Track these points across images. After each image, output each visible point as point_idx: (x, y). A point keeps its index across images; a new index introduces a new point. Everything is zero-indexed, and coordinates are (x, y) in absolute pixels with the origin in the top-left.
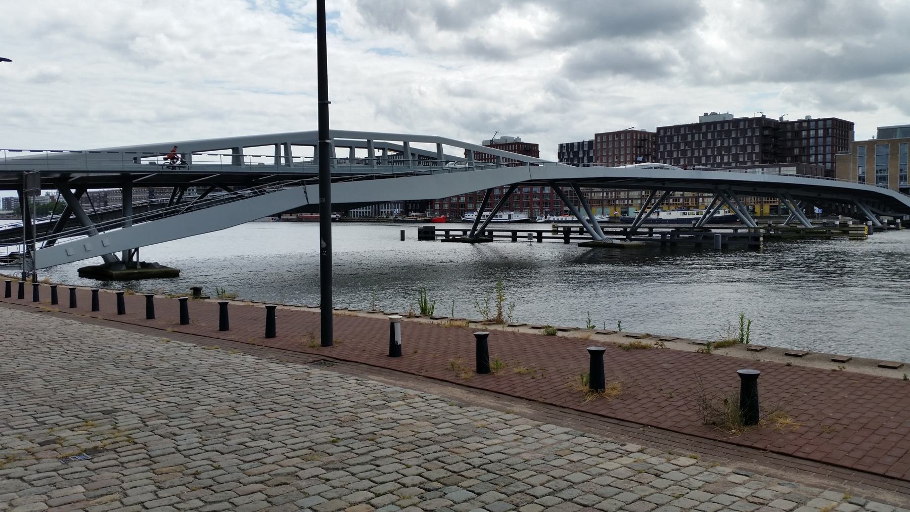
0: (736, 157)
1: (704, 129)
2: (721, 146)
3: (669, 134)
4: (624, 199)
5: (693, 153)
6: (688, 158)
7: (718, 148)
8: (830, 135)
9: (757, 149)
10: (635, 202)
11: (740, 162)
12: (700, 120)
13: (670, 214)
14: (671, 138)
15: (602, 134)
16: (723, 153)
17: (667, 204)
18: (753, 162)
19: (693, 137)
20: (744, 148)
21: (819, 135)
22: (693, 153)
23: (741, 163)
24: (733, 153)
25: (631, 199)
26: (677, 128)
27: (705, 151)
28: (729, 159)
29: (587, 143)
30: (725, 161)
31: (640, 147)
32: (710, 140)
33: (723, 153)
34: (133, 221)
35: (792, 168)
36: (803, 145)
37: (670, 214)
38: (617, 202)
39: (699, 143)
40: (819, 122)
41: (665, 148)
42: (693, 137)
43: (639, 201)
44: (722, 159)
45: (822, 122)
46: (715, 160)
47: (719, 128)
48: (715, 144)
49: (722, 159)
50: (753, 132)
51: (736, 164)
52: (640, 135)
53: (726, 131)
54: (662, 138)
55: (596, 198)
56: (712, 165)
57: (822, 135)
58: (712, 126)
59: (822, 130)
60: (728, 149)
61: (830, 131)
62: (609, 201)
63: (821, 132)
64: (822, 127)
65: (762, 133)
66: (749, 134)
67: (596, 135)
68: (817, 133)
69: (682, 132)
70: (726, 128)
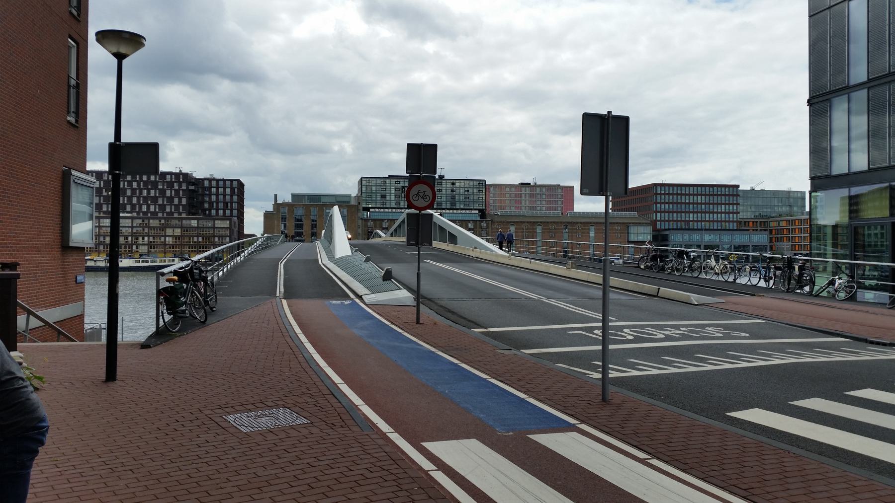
7: (144, 197)
8: (236, 193)
9: (184, 201)
11: (167, 213)
16: (149, 202)
17: (96, 251)
18: (180, 214)
20: (170, 200)
24: (159, 203)
28: (171, 209)
30: (151, 210)
32: (135, 189)
33: (149, 202)
36: (212, 200)
44: (148, 208)
45: (229, 182)
46: (141, 208)
48: (141, 193)
49: (148, 208)
50: (180, 186)
51: (163, 213)
53: (152, 182)
56: (138, 213)
59: (229, 189)
60: (155, 200)
61: (236, 190)
63: (228, 191)
65: (187, 187)
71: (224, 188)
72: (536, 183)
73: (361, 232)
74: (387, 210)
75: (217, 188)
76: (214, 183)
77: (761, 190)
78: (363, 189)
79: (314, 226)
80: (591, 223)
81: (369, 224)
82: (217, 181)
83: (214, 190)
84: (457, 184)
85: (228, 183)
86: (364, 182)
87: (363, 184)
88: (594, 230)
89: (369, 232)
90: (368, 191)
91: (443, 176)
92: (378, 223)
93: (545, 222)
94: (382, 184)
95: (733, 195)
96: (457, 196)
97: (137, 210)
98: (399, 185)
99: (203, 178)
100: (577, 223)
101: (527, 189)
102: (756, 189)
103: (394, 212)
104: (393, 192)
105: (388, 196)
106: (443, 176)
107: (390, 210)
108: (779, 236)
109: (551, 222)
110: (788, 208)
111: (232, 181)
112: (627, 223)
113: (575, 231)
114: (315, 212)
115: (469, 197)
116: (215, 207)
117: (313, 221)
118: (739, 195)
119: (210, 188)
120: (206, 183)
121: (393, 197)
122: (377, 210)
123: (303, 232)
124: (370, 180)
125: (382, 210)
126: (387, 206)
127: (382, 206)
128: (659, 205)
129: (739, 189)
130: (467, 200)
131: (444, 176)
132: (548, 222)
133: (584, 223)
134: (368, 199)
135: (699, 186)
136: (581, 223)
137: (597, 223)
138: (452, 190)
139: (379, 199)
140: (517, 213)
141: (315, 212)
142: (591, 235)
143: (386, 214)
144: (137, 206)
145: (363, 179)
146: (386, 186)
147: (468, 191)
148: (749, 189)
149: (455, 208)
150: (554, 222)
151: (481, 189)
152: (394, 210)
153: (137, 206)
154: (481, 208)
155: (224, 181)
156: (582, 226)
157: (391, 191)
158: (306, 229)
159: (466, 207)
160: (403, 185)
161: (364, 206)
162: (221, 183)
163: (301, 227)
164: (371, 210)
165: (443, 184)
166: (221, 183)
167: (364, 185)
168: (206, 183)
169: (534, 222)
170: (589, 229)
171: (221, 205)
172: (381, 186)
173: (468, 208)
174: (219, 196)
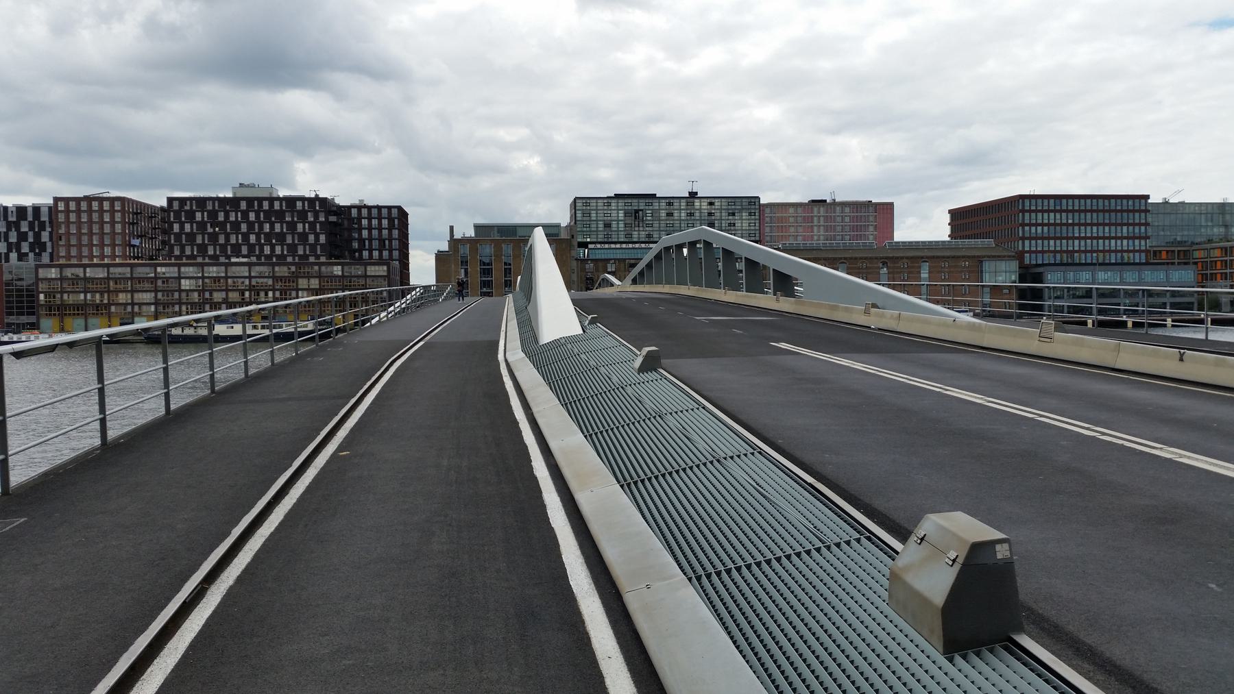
0: (203, 249)
1: (243, 205)
2: (270, 232)
3: (187, 208)
4: (126, 305)
5: (227, 239)
6: (310, 245)
7: (266, 234)
8: (396, 226)
9: (323, 238)
10: (144, 308)
11: (300, 256)
12: (234, 193)
13: (232, 327)
14: (191, 216)
15: (68, 198)
16: (274, 241)
18: (318, 257)
19: (227, 216)
20: (303, 237)
21: (383, 226)
22: (227, 239)
23: (211, 257)
25: (136, 304)
26: (201, 202)
27: (246, 237)
28: (305, 250)
29: (14, 209)
30: (277, 253)
31: (133, 224)
34: (1041, 298)
35: (381, 268)
36: (364, 237)
37: (232, 327)
38: (113, 309)
39: (236, 226)
40: (383, 210)
41: (182, 228)
42: (227, 216)
43: (153, 308)
44: (273, 250)
45: (386, 209)
46: (262, 250)
47: (266, 205)
48: (261, 228)
49: (273, 250)
50: (316, 216)
52: (137, 205)
54: (178, 214)
55: (71, 302)
56: (259, 257)
57: (387, 226)
58: (256, 203)
59: (386, 220)
60: (281, 238)
61: (396, 221)
62: (97, 307)
63: (385, 223)
64: (376, 216)
65: (327, 218)
66: (311, 219)
67: (56, 200)
68: (380, 223)
69: (210, 207)
70: (187, 208)
71: (380, 219)
72: (834, 200)
73: (576, 279)
74: (613, 246)
75: (370, 219)
76: (365, 212)
77: (1179, 203)
78: (578, 215)
79: (508, 272)
80: (922, 258)
81: (587, 266)
82: (370, 208)
83: (365, 222)
84: (716, 204)
85: (385, 212)
86: (579, 204)
87: (577, 208)
89: (587, 279)
90: (585, 218)
91: (696, 193)
92: (600, 264)
93: (851, 258)
94: (606, 208)
95: (1140, 211)
96: (716, 222)
97: (257, 253)
98: (630, 208)
99: (349, 205)
100: (902, 258)
101: (822, 209)
102: (1171, 201)
103: (642, 248)
104: (622, 218)
105: (614, 225)
106: (696, 193)
107: (618, 246)
108: (1209, 272)
109: (861, 258)
110: (1222, 230)
111: (389, 208)
112: (978, 257)
113: (898, 270)
114: (508, 249)
115: (734, 224)
116: (387, 247)
117: (505, 264)
118: (1149, 211)
119: (360, 218)
120: (354, 212)
121: (621, 225)
122: (599, 246)
123: (492, 281)
125: (607, 246)
126: (614, 240)
127: (606, 240)
129: (1150, 201)
131: (697, 193)
132: (856, 258)
133: (912, 258)
134: (585, 229)
135: (1083, 198)
136: (907, 258)
137: (933, 257)
138: (709, 213)
140: (973, 243)
141: (508, 249)
142: (922, 275)
143: (611, 251)
144: (257, 247)
145: (577, 201)
148: (1161, 202)
150: (866, 258)
152: (624, 246)
153: (257, 247)
155: (379, 208)
158: (497, 276)
160: (636, 208)
161: (580, 240)
162: (375, 212)
163: (489, 274)
164: (591, 246)
165: (696, 204)
166: (375, 212)
167: (579, 210)
168: (354, 212)
169: (835, 259)
170: (920, 267)
171: (375, 244)
172: (604, 210)
174: (373, 231)
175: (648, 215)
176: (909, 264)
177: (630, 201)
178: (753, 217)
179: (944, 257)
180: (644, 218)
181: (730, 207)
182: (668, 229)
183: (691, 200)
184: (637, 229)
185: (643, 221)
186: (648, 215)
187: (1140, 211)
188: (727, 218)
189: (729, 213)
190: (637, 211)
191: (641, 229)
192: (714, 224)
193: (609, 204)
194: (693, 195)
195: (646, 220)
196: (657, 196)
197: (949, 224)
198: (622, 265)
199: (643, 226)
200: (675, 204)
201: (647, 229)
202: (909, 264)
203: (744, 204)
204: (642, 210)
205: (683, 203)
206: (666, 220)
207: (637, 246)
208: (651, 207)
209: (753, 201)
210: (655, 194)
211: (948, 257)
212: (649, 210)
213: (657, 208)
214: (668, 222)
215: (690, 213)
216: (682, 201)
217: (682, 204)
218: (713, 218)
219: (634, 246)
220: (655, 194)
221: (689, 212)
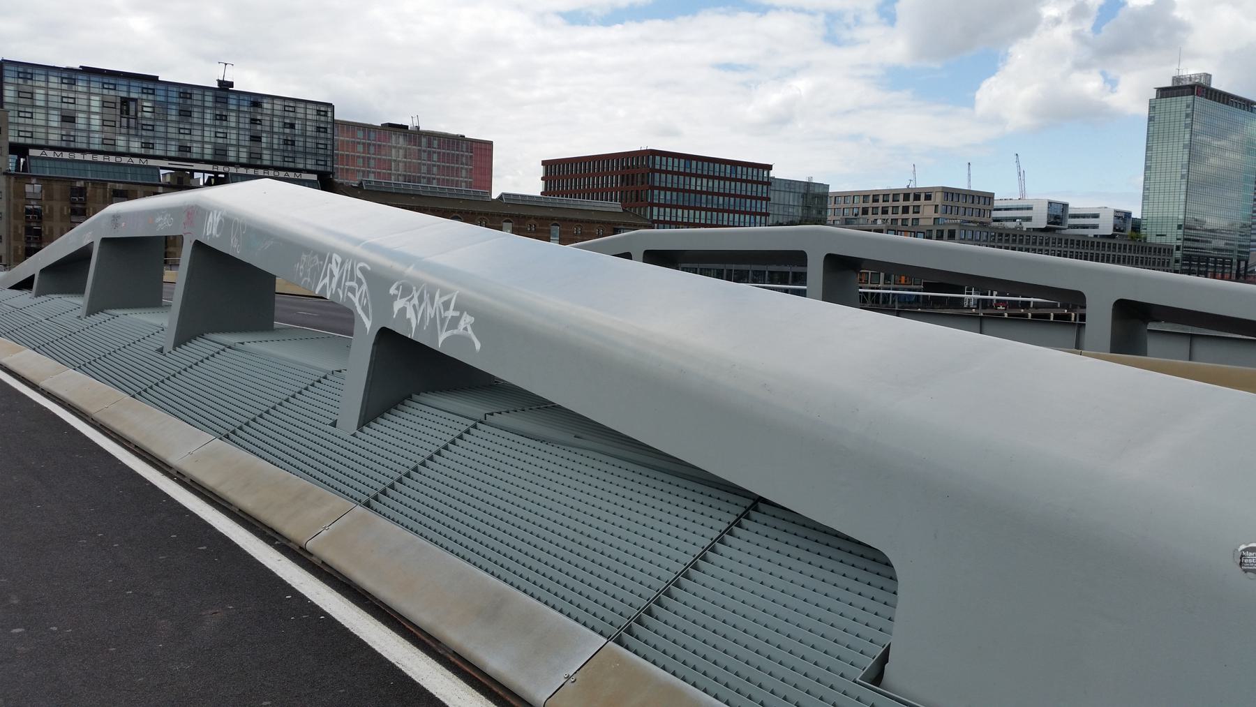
74: (78, 156)
80: (553, 219)
81: (28, 188)
88: (558, 234)
89: (28, 211)
90: (22, 101)
91: (231, 84)
94: (65, 86)
95: (763, 183)
96: (264, 135)
98: (112, 93)
100: (530, 217)
104: (97, 110)
105: (81, 120)
106: (231, 84)
107: (89, 157)
112: (615, 223)
121: (96, 121)
122: (50, 154)
124: (30, 71)
125: (66, 155)
126: (79, 146)
127: (64, 144)
128: (656, 192)
130: (290, 148)
133: (541, 218)
134: (21, 120)
136: (536, 218)
137: (565, 220)
139: (55, 124)
146: (76, 92)
147: (292, 126)
149: (259, 163)
150: (486, 214)
151: (322, 125)
152: (100, 158)
154: (321, 168)
156: (538, 225)
157: (89, 106)
159: (286, 165)
160: (124, 95)
161: (11, 139)
164: (33, 152)
165: (231, 101)
173: (292, 165)
175: (145, 109)
176: (538, 227)
177: (112, 81)
178: (322, 135)
179: (577, 221)
180: (139, 115)
181: (286, 114)
182: (181, 137)
183: (223, 94)
184: (124, 131)
185: (136, 118)
186: (145, 109)
187: (763, 183)
188: (281, 130)
189: (285, 123)
190: (125, 101)
191: (132, 132)
192: (260, 138)
193: (72, 82)
194: (225, 86)
195: (143, 118)
196: (160, 79)
197: (542, 179)
198: (100, 191)
199: (136, 128)
200: (195, 97)
201: (144, 133)
202: (538, 227)
203: (309, 111)
204: (135, 100)
205: (209, 99)
206: (179, 122)
207: (125, 160)
208: (151, 97)
209: (322, 109)
210: (158, 77)
211: (582, 221)
212: (148, 101)
213: (162, 99)
214: (181, 126)
215: (221, 115)
216: (207, 93)
217: (207, 98)
218: (259, 127)
219: (119, 159)
220: (158, 77)
221: (218, 113)
